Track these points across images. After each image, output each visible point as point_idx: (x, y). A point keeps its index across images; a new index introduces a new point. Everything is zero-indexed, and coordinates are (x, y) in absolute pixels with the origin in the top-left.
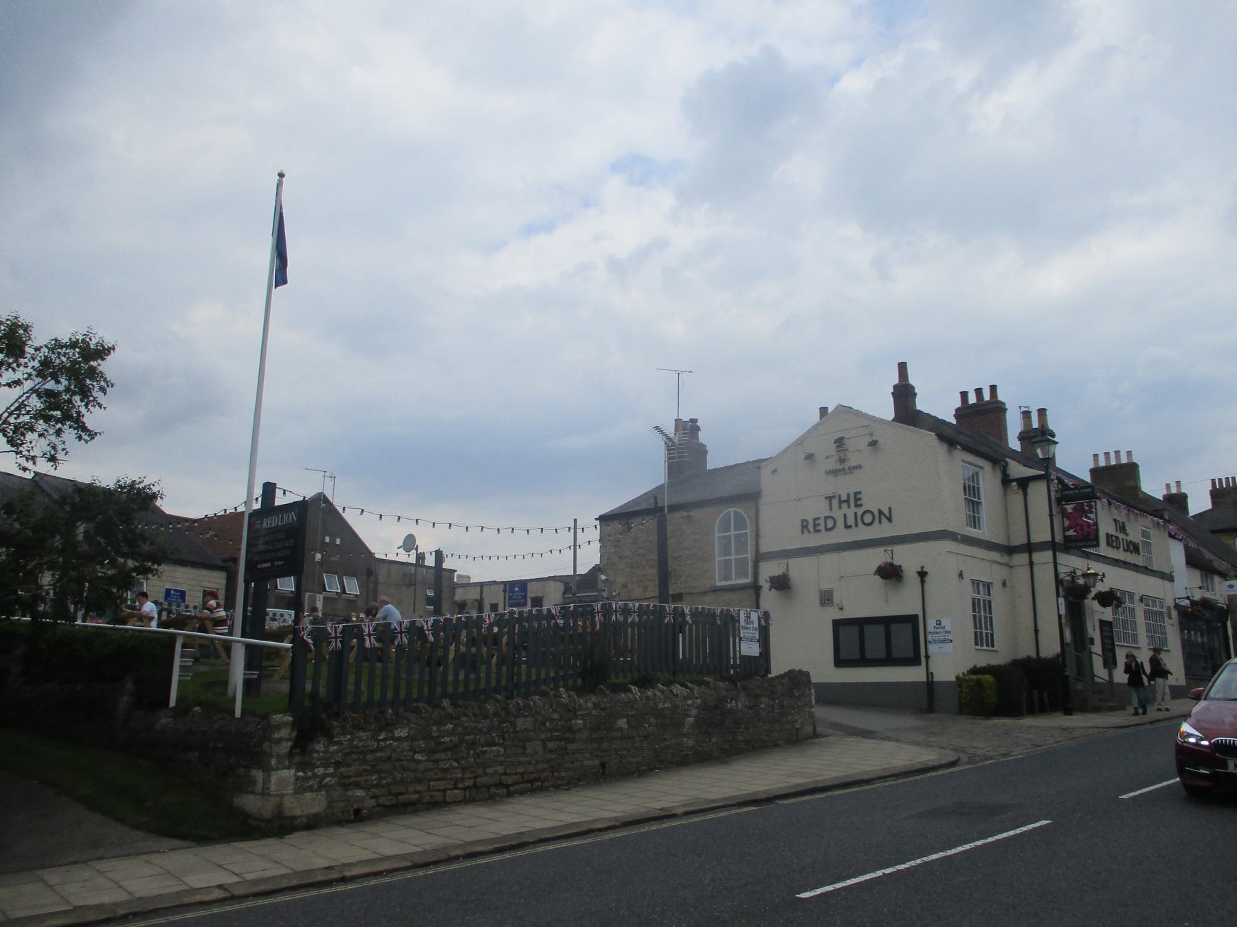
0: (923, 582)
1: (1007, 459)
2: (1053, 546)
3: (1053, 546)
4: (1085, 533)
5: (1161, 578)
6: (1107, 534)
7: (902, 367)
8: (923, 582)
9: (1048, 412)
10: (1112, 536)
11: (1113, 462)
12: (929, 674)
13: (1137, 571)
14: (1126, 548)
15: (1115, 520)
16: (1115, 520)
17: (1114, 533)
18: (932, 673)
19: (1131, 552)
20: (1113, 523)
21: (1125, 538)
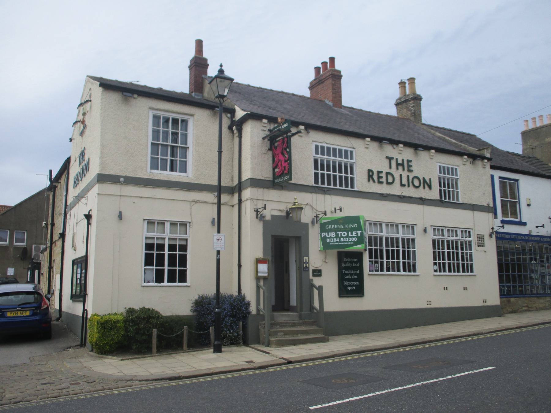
0: (89, 224)
1: (237, 108)
2: (255, 183)
3: (255, 183)
4: (283, 168)
5: (471, 210)
6: (370, 171)
7: (199, 44)
8: (89, 224)
9: (416, 81)
10: (379, 172)
11: (538, 124)
12: (85, 310)
13: (423, 204)
14: (405, 182)
15: (390, 159)
16: (390, 159)
17: (385, 169)
18: (86, 310)
19: (416, 187)
20: (388, 161)
21: (405, 174)
